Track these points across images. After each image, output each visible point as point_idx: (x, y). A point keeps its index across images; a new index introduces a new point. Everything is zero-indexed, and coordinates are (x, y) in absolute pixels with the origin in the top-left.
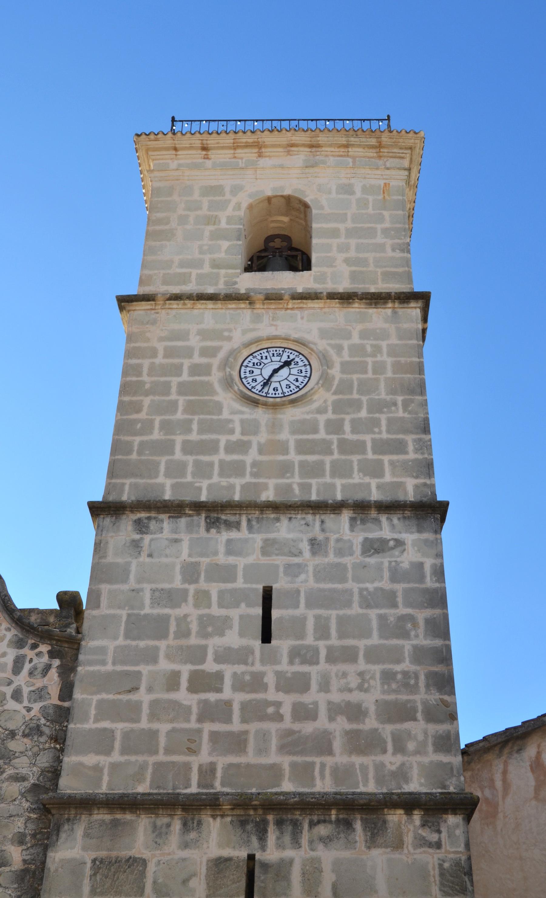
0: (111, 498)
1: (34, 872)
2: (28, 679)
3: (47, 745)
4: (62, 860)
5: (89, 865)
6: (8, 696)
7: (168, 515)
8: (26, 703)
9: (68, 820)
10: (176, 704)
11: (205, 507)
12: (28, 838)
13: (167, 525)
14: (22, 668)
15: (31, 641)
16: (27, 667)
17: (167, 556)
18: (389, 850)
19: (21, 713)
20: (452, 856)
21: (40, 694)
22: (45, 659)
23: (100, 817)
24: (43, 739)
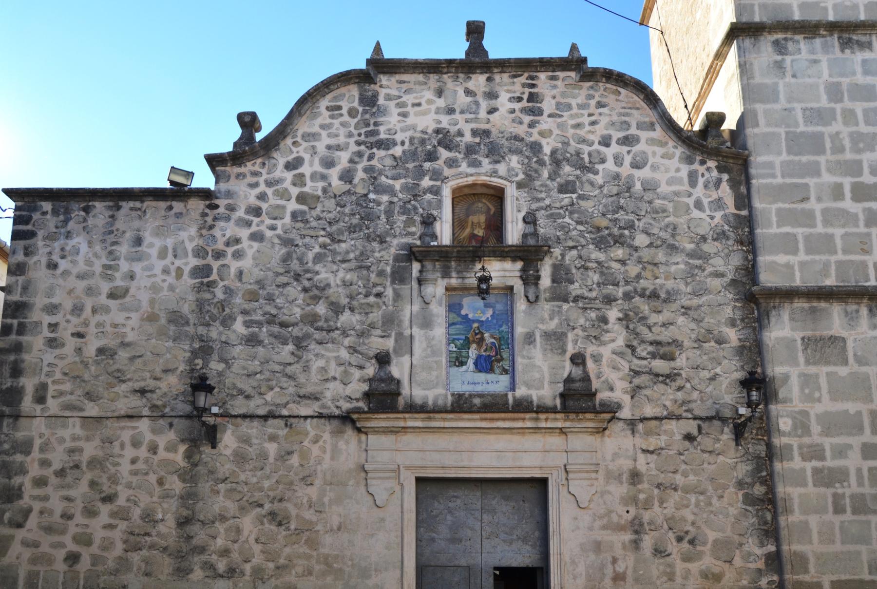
0: (744, 20)
1: (750, 348)
2: (704, 191)
3: (735, 248)
4: (776, 338)
5: (799, 342)
6: (692, 206)
7: (803, 36)
8: (708, 212)
9: (774, 307)
10: (844, 212)
11: (840, 27)
12: (738, 322)
13: (803, 45)
14: (697, 181)
15: (698, 158)
16: (701, 181)
17: (809, 76)
19: (708, 220)
21: (719, 204)
22: (715, 173)
23: (800, 305)
24: (730, 242)
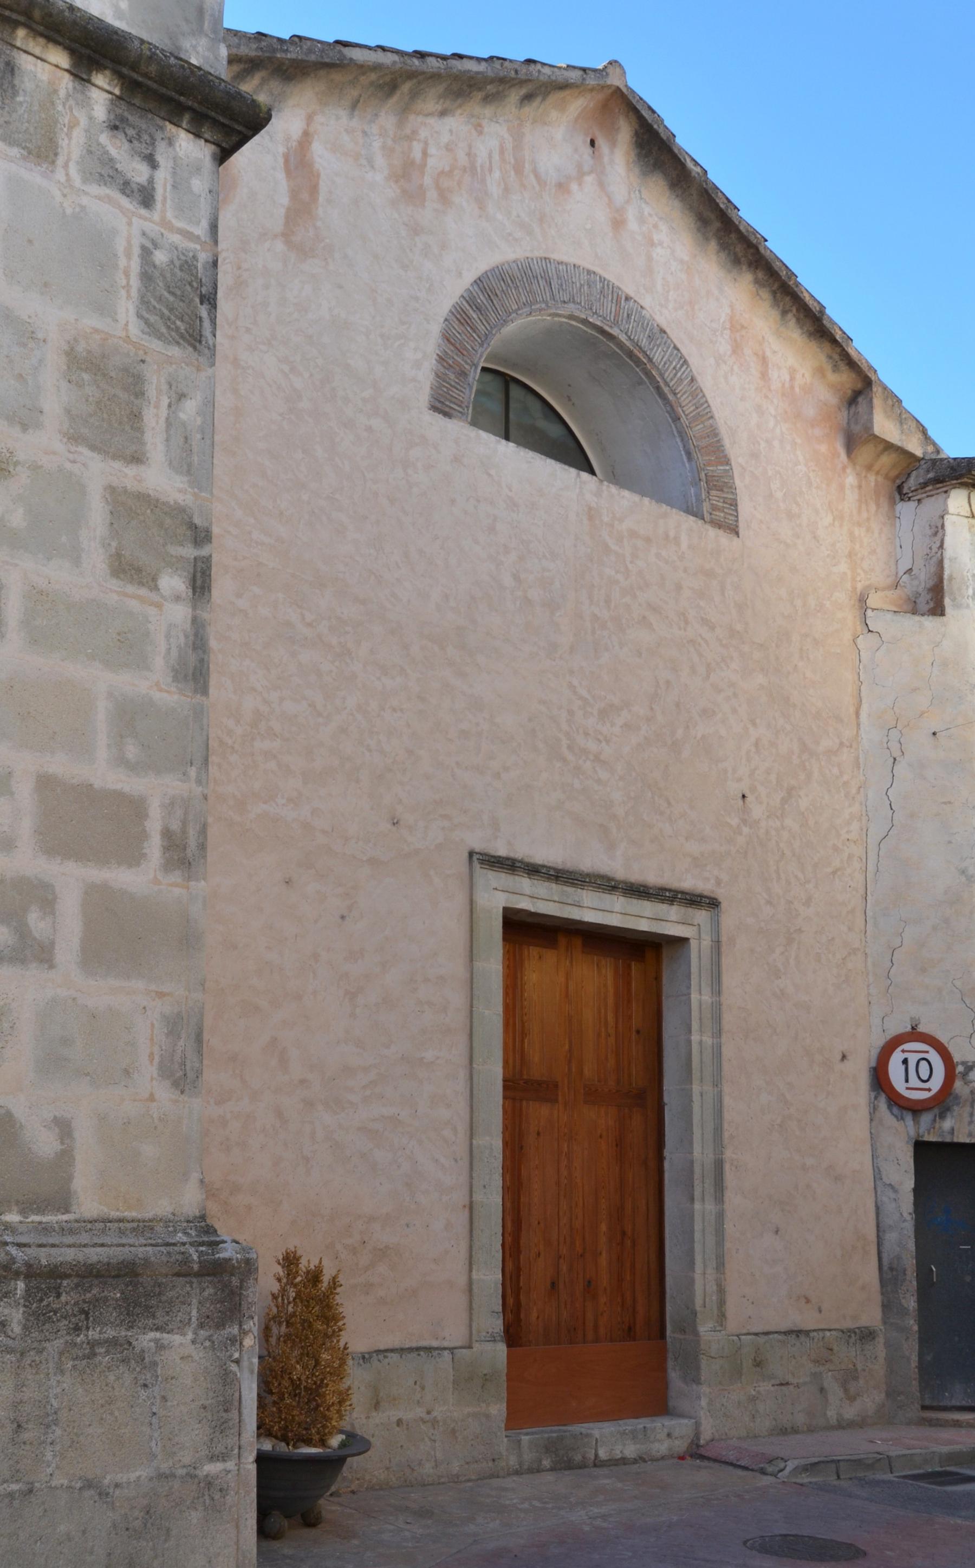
18: (15, 152)
20: (176, 238)
